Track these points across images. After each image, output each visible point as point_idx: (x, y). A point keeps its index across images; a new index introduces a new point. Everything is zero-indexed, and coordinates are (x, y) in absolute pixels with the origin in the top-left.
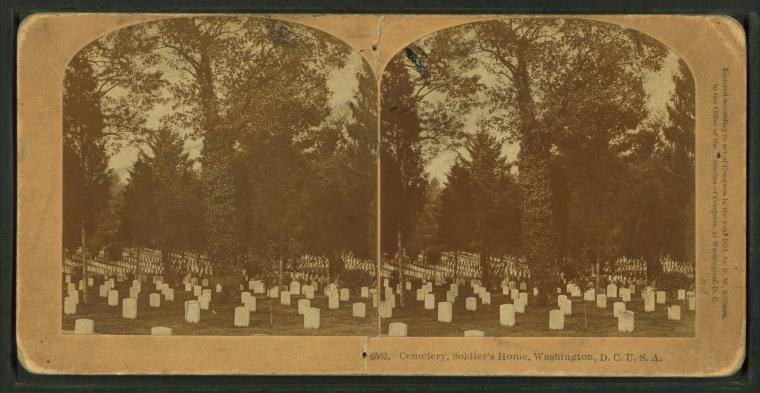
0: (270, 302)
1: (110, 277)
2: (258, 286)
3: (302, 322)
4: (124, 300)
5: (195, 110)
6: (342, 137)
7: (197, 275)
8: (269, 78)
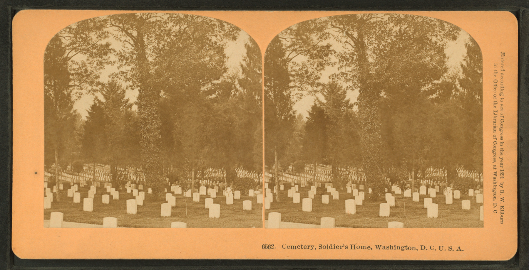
0: (404, 200)
1: (295, 184)
2: (396, 189)
3: (426, 213)
4: (304, 200)
5: (353, 70)
6: (455, 87)
7: (356, 183)
8: (405, 48)
